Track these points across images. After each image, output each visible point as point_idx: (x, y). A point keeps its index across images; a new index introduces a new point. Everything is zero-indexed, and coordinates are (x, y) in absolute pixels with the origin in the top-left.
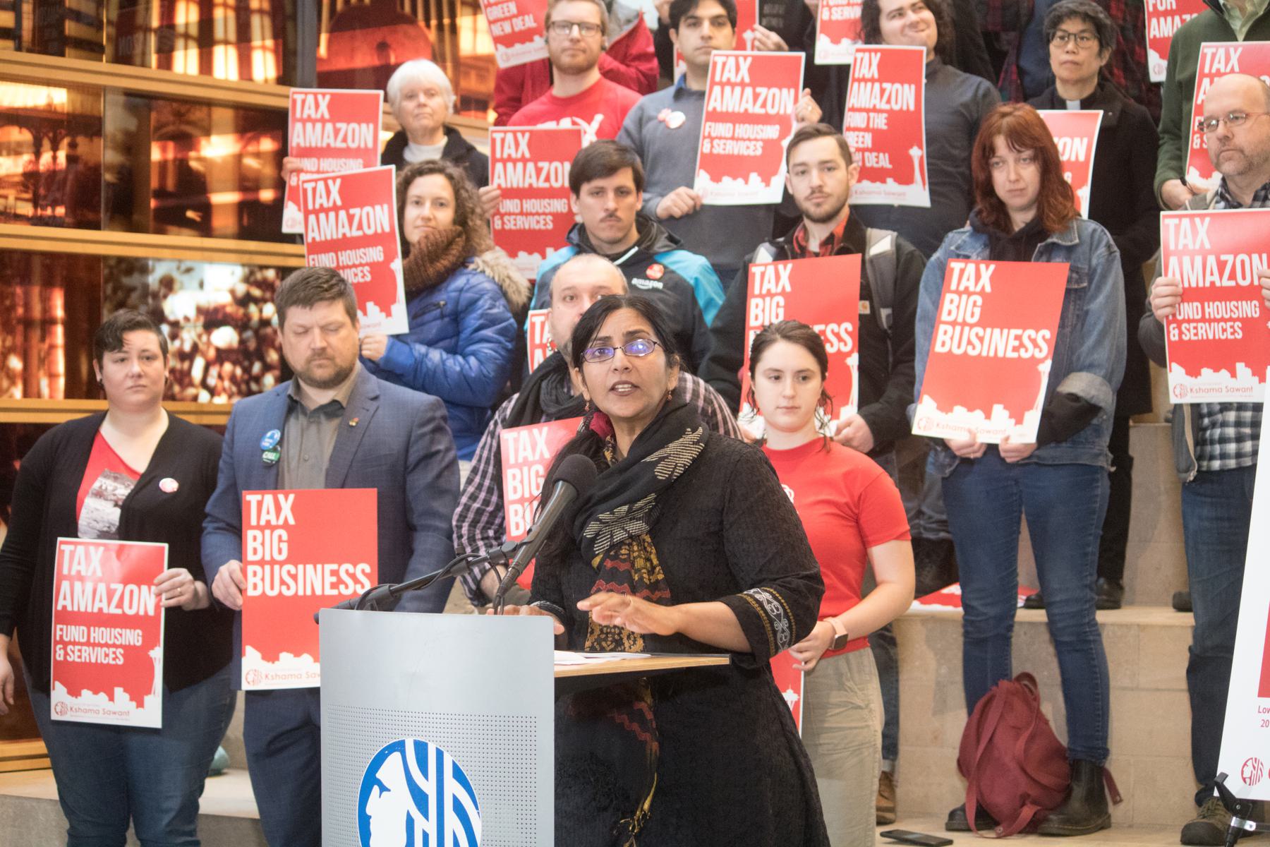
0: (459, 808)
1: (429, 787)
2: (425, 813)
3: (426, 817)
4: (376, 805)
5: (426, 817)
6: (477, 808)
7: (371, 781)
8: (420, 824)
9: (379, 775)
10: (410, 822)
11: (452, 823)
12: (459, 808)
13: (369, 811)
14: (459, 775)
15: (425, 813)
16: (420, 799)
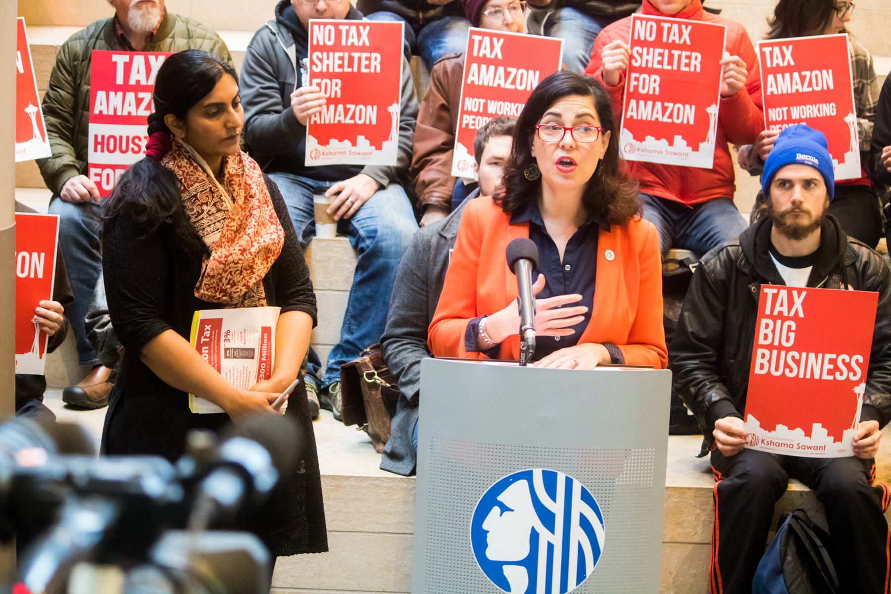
0: (585, 523)
1: (557, 508)
2: (551, 528)
3: (552, 531)
4: (493, 521)
5: (552, 531)
6: (602, 522)
7: (490, 501)
8: (545, 536)
9: (500, 498)
10: (534, 537)
11: (578, 535)
12: (585, 523)
13: (485, 526)
14: (586, 497)
15: (551, 528)
16: (547, 518)
